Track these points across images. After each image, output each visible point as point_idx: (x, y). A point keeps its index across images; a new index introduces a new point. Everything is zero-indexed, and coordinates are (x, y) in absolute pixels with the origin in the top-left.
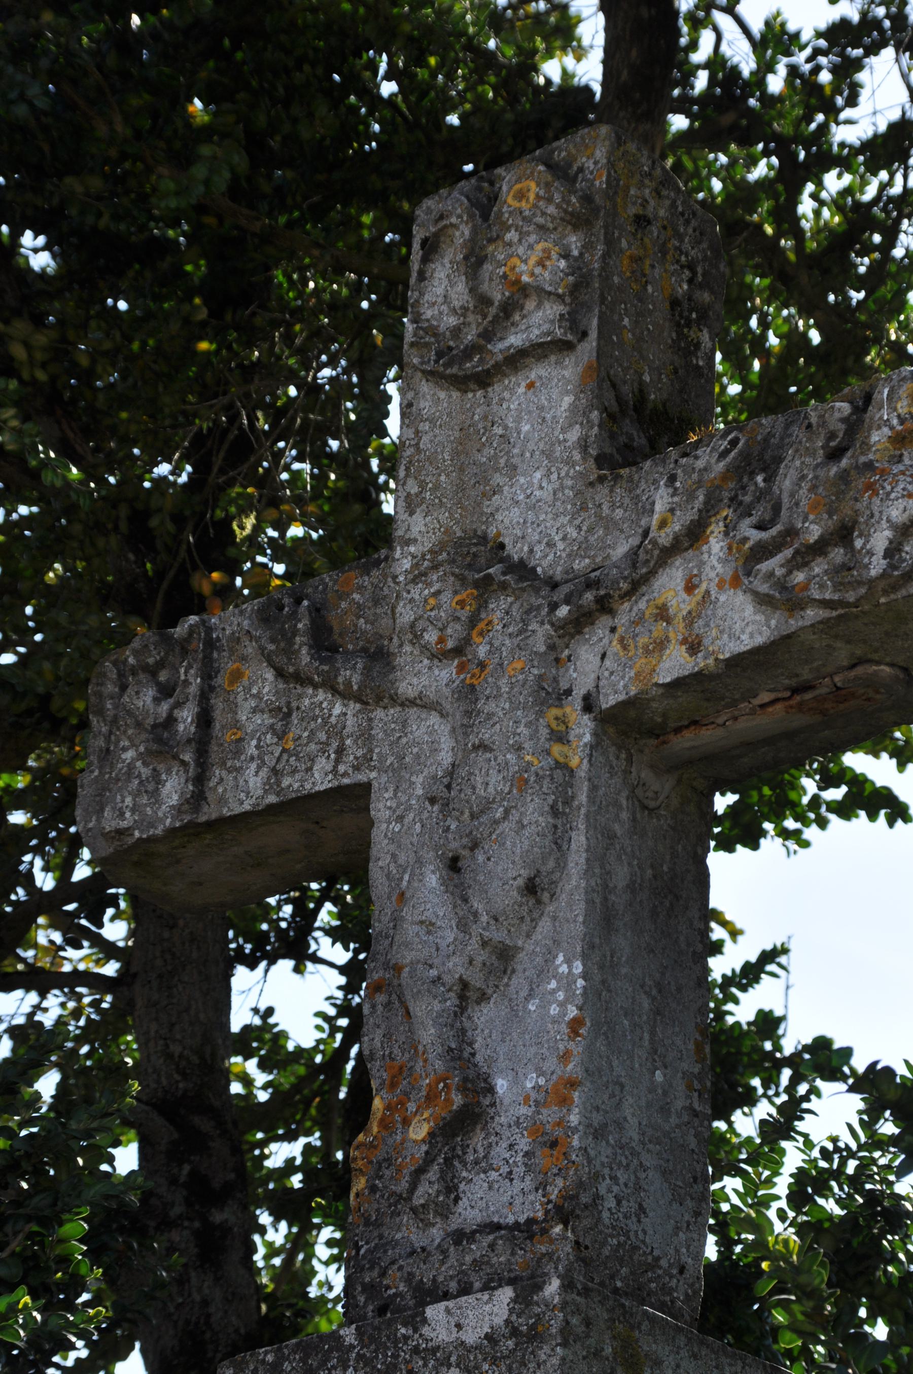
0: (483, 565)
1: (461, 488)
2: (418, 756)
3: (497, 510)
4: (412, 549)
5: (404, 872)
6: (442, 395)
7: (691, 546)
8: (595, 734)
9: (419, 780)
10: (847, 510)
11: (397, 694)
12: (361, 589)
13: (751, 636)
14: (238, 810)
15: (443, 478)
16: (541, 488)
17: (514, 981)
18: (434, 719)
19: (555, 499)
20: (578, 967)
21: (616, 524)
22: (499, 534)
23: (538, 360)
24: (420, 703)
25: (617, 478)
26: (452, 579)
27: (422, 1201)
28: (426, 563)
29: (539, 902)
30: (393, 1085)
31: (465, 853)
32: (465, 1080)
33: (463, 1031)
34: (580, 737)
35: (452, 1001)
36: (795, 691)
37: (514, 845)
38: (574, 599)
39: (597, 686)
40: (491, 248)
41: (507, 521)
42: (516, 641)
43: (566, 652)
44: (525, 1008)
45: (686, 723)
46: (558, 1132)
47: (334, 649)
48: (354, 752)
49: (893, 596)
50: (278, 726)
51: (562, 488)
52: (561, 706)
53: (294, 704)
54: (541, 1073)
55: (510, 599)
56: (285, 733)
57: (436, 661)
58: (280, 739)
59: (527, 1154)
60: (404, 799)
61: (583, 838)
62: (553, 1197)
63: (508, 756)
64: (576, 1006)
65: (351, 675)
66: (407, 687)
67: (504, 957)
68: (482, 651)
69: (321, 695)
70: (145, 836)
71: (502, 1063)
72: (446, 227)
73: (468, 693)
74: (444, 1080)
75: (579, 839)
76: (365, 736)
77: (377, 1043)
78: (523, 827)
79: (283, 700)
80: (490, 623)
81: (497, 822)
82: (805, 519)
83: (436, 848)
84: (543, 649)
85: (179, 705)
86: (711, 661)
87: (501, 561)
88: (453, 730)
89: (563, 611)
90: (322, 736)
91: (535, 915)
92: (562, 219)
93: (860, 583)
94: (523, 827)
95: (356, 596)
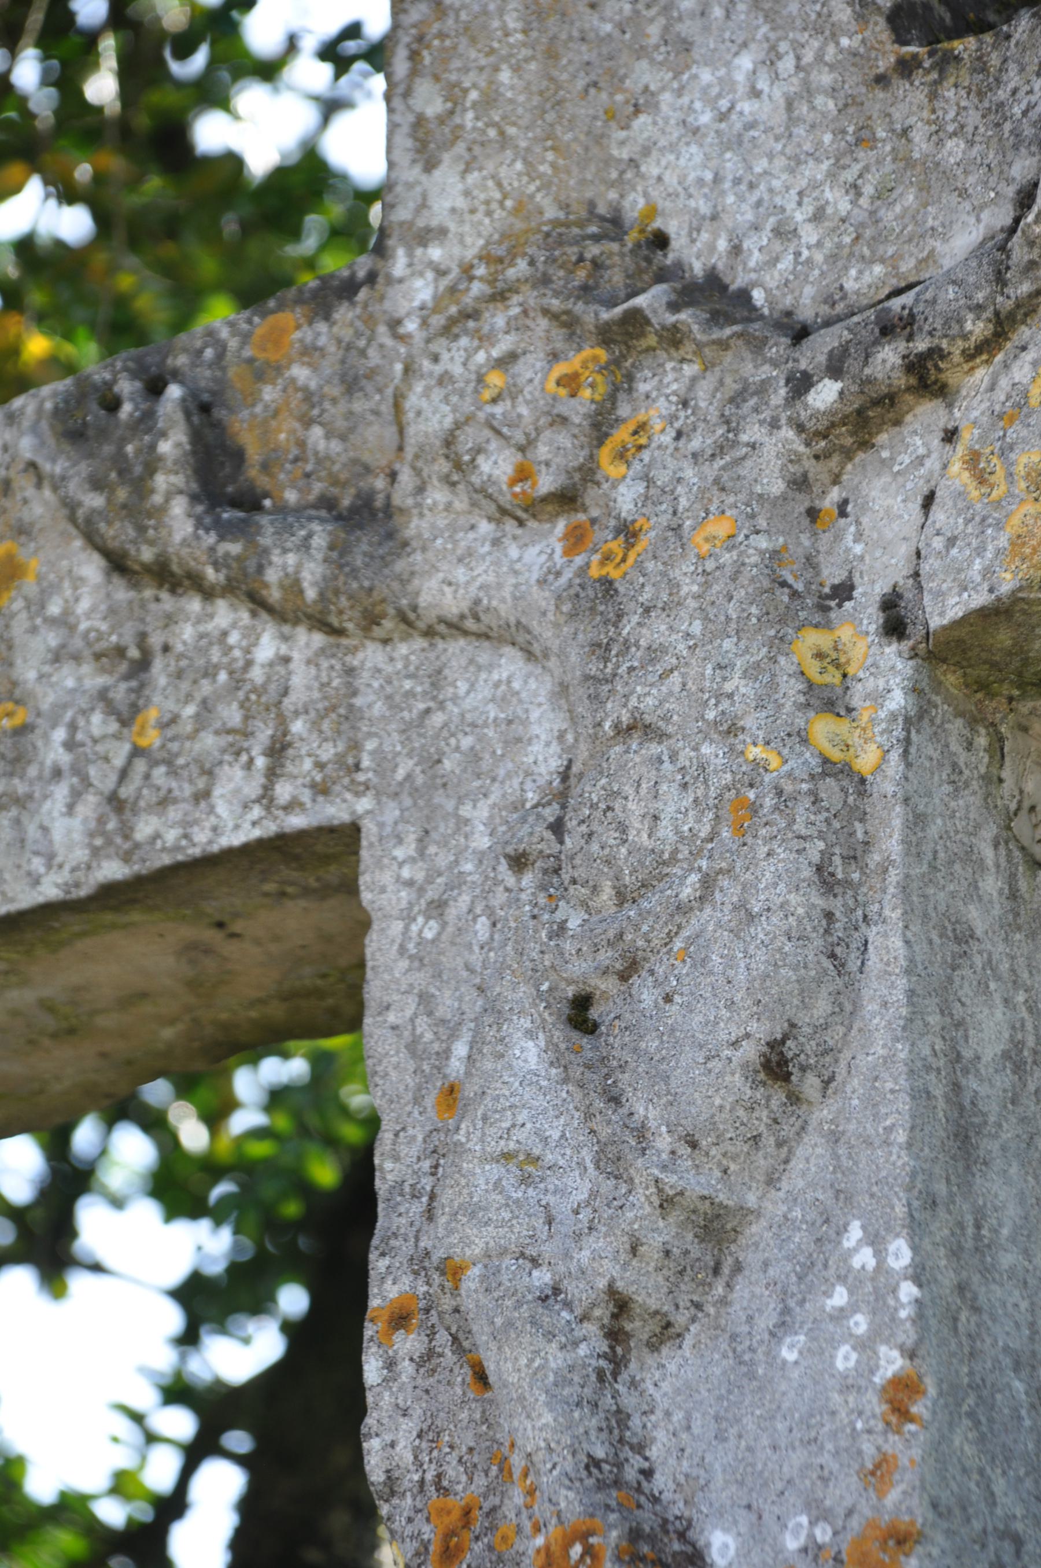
0: (624, 289)
1: (551, 99)
2: (474, 756)
3: (646, 151)
4: (435, 253)
5: (453, 1035)
8: (915, 690)
9: (479, 813)
12: (310, 352)
15: (505, 76)
16: (755, 93)
17: (741, 1291)
18: (510, 665)
19: (792, 121)
20: (900, 1254)
21: (947, 176)
22: (652, 211)
25: (946, 62)
26: (544, 323)
28: (477, 288)
29: (794, 1098)
31: (609, 985)
32: (635, 1535)
33: (621, 1417)
34: (878, 698)
35: (592, 1343)
37: (730, 962)
38: (852, 365)
39: (916, 575)
41: (671, 179)
42: (712, 470)
43: (835, 494)
44: (772, 1357)
47: (250, 502)
48: (313, 748)
50: (120, 693)
51: (808, 91)
52: (827, 625)
53: (156, 640)
54: (820, 1514)
55: (690, 370)
56: (135, 709)
57: (510, 526)
58: (125, 722)
60: (443, 860)
61: (896, 943)
65: (299, 562)
66: (440, 591)
68: (626, 498)
69: (225, 614)
71: (721, 1491)
73: (599, 599)
74: (583, 1536)
75: (888, 945)
76: (340, 711)
77: (404, 1454)
78: (751, 918)
79: (127, 635)
80: (641, 428)
81: (683, 909)
83: (536, 975)
84: (777, 487)
87: (661, 277)
88: (563, 689)
89: (825, 394)
90: (232, 714)
91: (787, 1130)
94: (751, 918)
95: (300, 373)
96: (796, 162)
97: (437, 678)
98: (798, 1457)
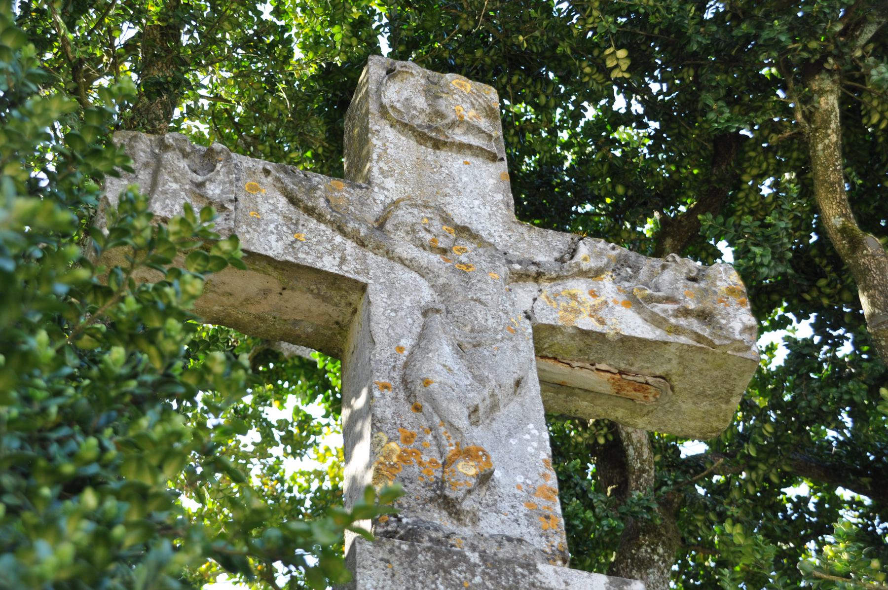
2: (405, 288)
3: (449, 204)
4: (386, 193)
6: (404, 138)
10: (708, 305)
11: (393, 251)
14: (262, 252)
17: (494, 423)
18: (414, 275)
24: (408, 264)
27: (468, 509)
29: (515, 392)
36: (621, 373)
40: (443, 95)
45: (551, 356)
46: (547, 512)
49: (735, 353)
53: (301, 222)
59: (526, 515)
60: (395, 302)
62: (556, 544)
63: (501, 314)
67: (494, 407)
69: (322, 227)
72: (407, 72)
78: (518, 350)
82: (685, 297)
85: (210, 180)
86: (612, 332)
92: (485, 108)
93: (726, 338)
97: (392, 268)
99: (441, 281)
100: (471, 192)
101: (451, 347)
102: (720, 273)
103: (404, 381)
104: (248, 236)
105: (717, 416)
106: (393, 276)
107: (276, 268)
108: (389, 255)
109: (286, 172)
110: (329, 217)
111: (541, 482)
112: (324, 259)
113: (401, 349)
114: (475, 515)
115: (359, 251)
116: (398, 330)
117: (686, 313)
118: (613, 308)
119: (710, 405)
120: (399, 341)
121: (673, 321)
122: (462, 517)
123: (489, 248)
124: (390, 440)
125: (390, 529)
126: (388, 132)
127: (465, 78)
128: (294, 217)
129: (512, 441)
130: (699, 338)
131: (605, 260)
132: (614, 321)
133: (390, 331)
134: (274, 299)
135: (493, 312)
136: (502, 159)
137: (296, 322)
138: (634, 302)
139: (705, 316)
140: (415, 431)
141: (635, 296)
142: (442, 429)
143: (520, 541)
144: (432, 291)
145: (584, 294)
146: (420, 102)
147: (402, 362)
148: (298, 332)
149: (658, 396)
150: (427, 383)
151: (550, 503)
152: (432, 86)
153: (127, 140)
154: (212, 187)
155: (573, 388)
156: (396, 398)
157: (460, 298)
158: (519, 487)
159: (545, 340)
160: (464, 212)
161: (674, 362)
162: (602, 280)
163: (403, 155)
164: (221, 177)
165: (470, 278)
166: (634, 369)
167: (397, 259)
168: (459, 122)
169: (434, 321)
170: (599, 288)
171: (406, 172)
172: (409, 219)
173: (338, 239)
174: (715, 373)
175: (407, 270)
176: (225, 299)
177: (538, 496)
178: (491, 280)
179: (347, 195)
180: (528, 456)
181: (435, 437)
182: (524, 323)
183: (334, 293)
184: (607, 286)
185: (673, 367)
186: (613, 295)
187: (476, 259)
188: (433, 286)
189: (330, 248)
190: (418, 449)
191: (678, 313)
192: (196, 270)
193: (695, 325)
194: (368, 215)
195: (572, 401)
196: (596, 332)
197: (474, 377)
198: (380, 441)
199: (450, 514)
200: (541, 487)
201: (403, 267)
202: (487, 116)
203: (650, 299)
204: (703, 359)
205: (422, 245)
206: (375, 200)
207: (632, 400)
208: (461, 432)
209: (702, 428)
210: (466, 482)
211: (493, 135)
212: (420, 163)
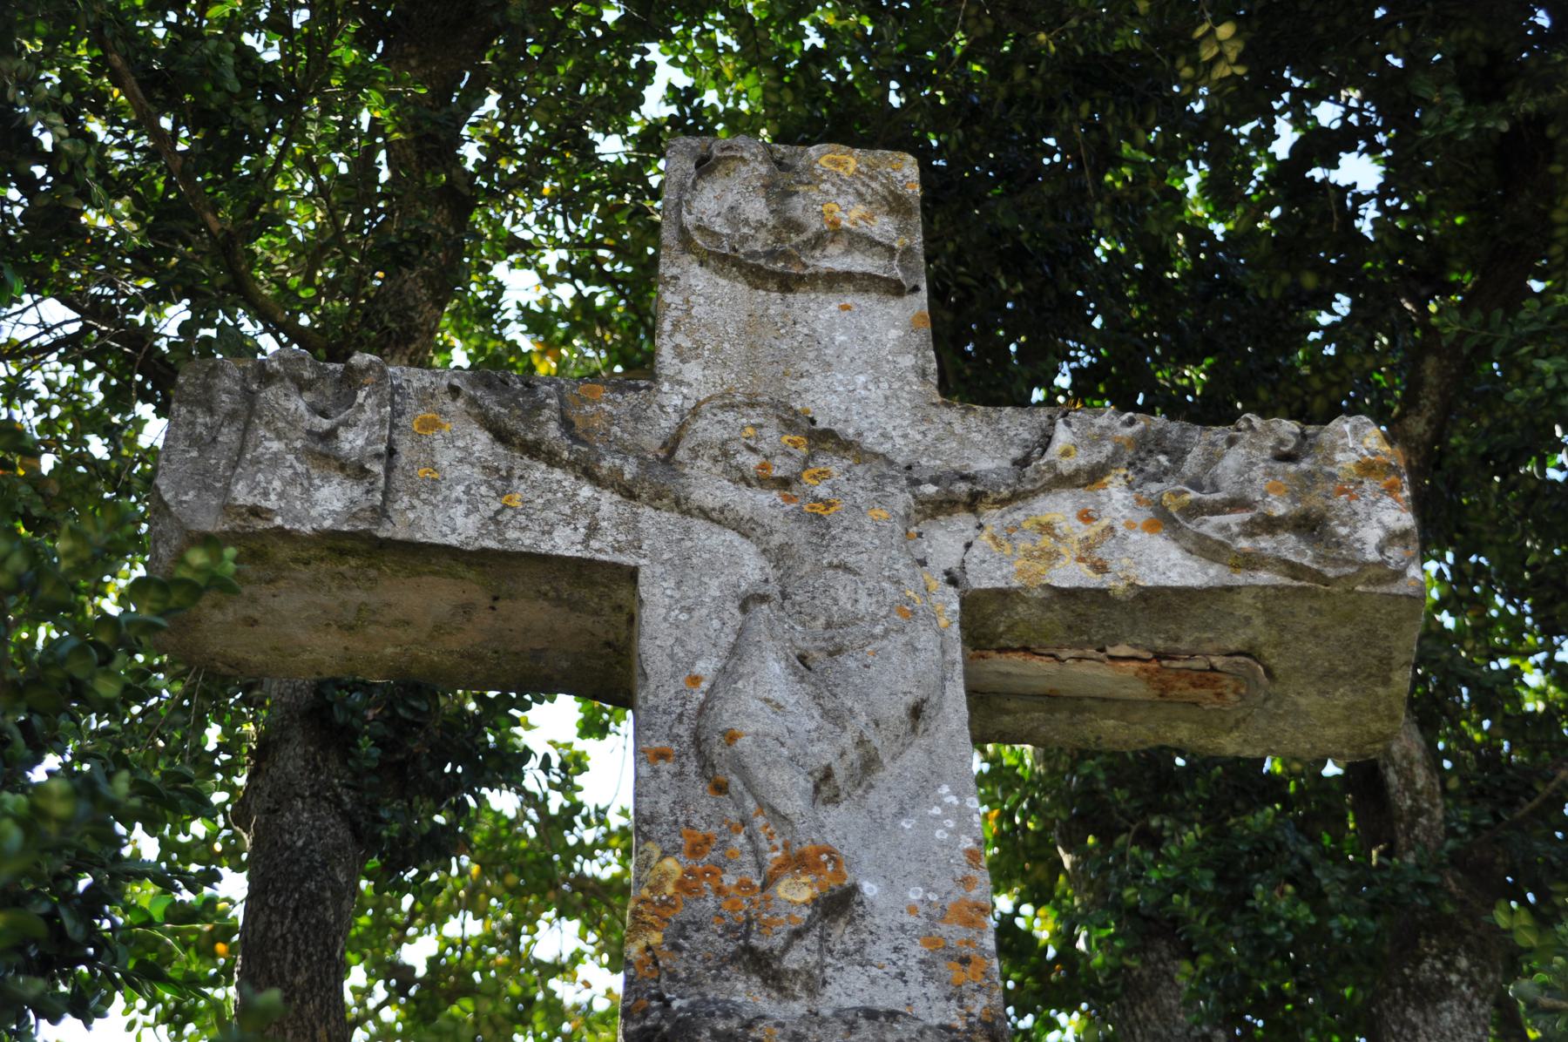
2: (710, 563)
3: (807, 390)
4: (685, 391)
6: (723, 282)
7: (1084, 486)
10: (1315, 502)
11: (687, 499)
13: (1182, 575)
14: (437, 539)
17: (872, 794)
18: (730, 536)
23: (857, 291)
26: (776, 421)
27: (796, 966)
29: (914, 729)
30: (695, 851)
36: (1159, 657)
39: (963, 568)
40: (801, 188)
45: (1016, 645)
46: (966, 951)
49: (1371, 589)
53: (517, 472)
59: (922, 962)
60: (691, 593)
62: (977, 1010)
63: (885, 585)
64: (975, 839)
67: (870, 763)
69: (558, 474)
70: (287, 527)
72: (733, 158)
76: (633, 524)
79: (503, 465)
82: (1265, 495)
85: (346, 424)
86: (1122, 585)
92: (884, 198)
93: (1347, 562)
96: (891, 417)
97: (687, 530)
98: (913, 866)
99: (777, 540)
100: (852, 360)
101: (783, 664)
102: (1344, 436)
103: (697, 740)
104: (411, 515)
105: (1375, 711)
106: (689, 544)
107: (469, 565)
108: (682, 506)
109: (489, 386)
110: (566, 454)
111: (959, 893)
112: (555, 534)
113: (695, 680)
114: (810, 976)
115: (626, 510)
116: (693, 645)
117: (1270, 525)
118: (1125, 537)
119: (1354, 691)
120: (693, 664)
121: (1244, 544)
122: (787, 984)
123: (875, 462)
124: (665, 854)
125: (649, 1023)
126: (695, 276)
127: (845, 149)
128: (503, 465)
129: (906, 824)
130: (1294, 570)
131: (1108, 448)
132: (1125, 562)
133: (677, 649)
134: (483, 619)
135: (870, 584)
136: (916, 289)
137: (536, 655)
138: (1164, 520)
139: (1310, 525)
140: (714, 829)
141: (1165, 509)
142: (760, 821)
143: (892, 1015)
144: (762, 562)
145: (1067, 519)
146: (757, 209)
147: (696, 704)
148: (545, 671)
149: (1243, 691)
150: (731, 737)
151: (973, 933)
152: (780, 175)
153: (202, 376)
154: (351, 436)
155: (1079, 699)
156: (681, 773)
157: (807, 567)
158: (912, 910)
159: (985, 620)
160: (835, 400)
161: (1258, 622)
162: (1104, 487)
163: (721, 313)
164: (367, 415)
165: (828, 527)
166: (1183, 646)
167: (696, 512)
168: (834, 233)
169: (755, 618)
170: (1099, 504)
171: (726, 345)
172: (718, 433)
173: (586, 491)
174: (1345, 631)
175: (716, 528)
176: (399, 632)
177: (950, 922)
178: (870, 522)
179: (608, 408)
180: (936, 848)
181: (749, 837)
182: (944, 593)
183: (585, 592)
184: (1116, 497)
185: (1258, 631)
186: (1126, 512)
187: (846, 488)
188: (764, 551)
189: (568, 512)
190: (717, 864)
191: (1250, 530)
192: (151, 609)
193: (1288, 546)
194: (647, 438)
195: (1084, 722)
196: (1089, 590)
197: (825, 713)
198: (649, 858)
199: (765, 981)
200: (957, 904)
201: (708, 524)
202: (891, 211)
203: (1196, 510)
204: (1311, 608)
205: (744, 479)
206: (661, 407)
207: (1196, 704)
208: (791, 823)
209: (1351, 738)
210: (790, 916)
211: (896, 245)
212: (754, 324)
